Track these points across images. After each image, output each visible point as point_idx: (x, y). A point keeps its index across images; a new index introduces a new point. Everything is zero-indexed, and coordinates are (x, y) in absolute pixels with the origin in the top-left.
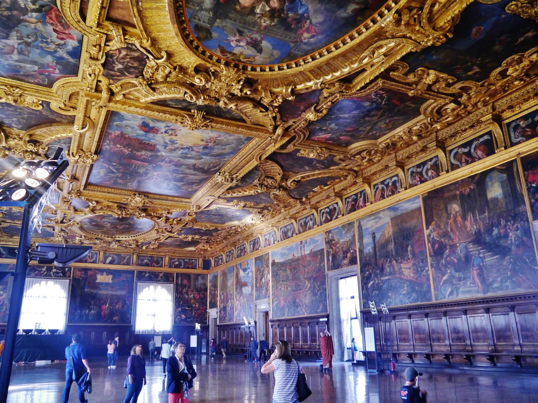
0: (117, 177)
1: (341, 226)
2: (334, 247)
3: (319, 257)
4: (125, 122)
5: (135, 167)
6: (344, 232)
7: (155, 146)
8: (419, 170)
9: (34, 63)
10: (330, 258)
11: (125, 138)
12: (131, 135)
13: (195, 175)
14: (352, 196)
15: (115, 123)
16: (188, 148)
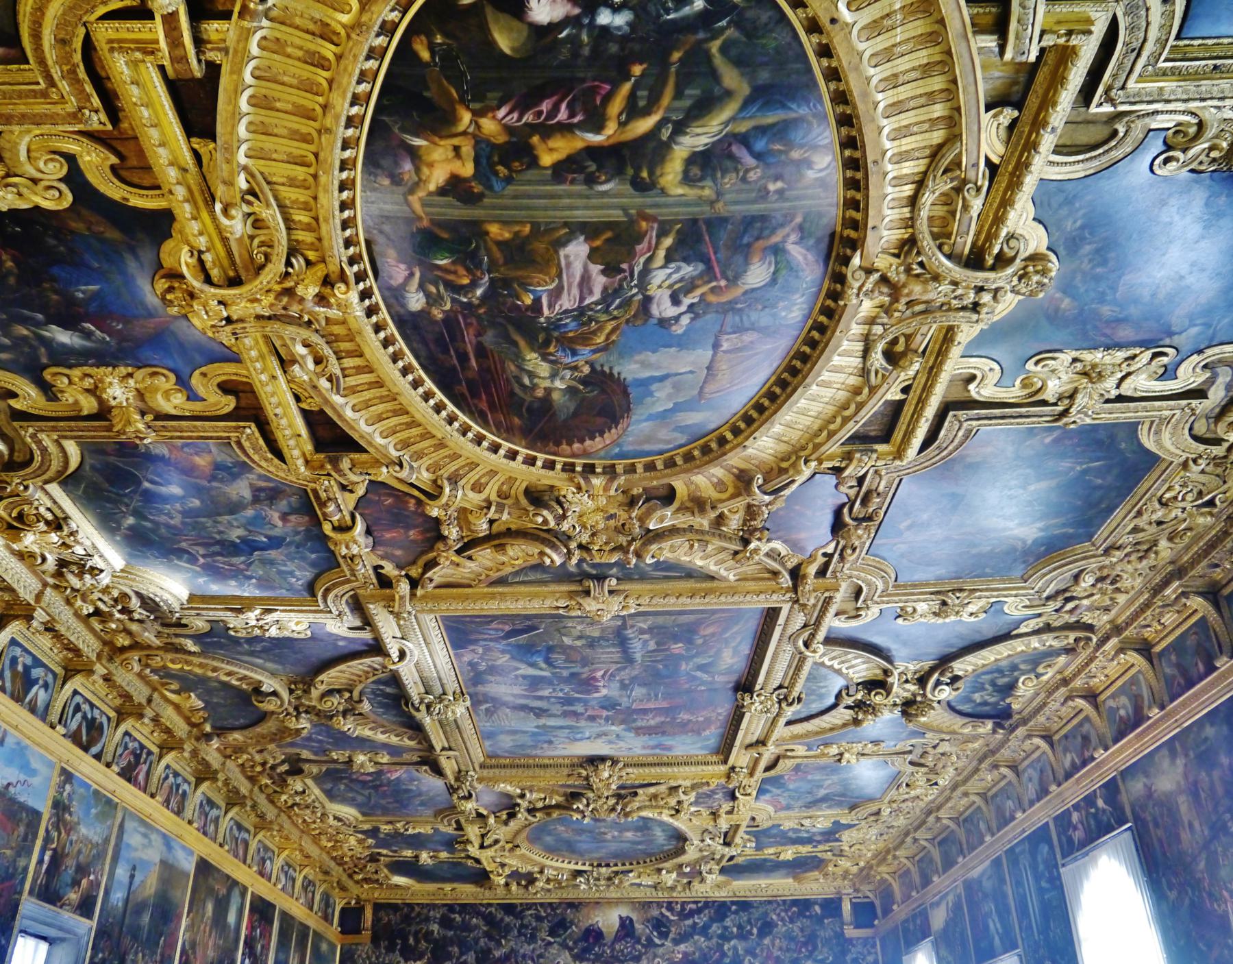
0: (689, 659)
1: (95, 786)
2: (63, 834)
3: (22, 829)
4: (699, 745)
5: (656, 696)
6: (93, 811)
7: (638, 734)
8: (207, 809)
9: (810, 781)
10: (47, 858)
11: (693, 731)
12: (684, 737)
13: (515, 696)
14: (135, 739)
15: (713, 741)
16: (576, 740)
